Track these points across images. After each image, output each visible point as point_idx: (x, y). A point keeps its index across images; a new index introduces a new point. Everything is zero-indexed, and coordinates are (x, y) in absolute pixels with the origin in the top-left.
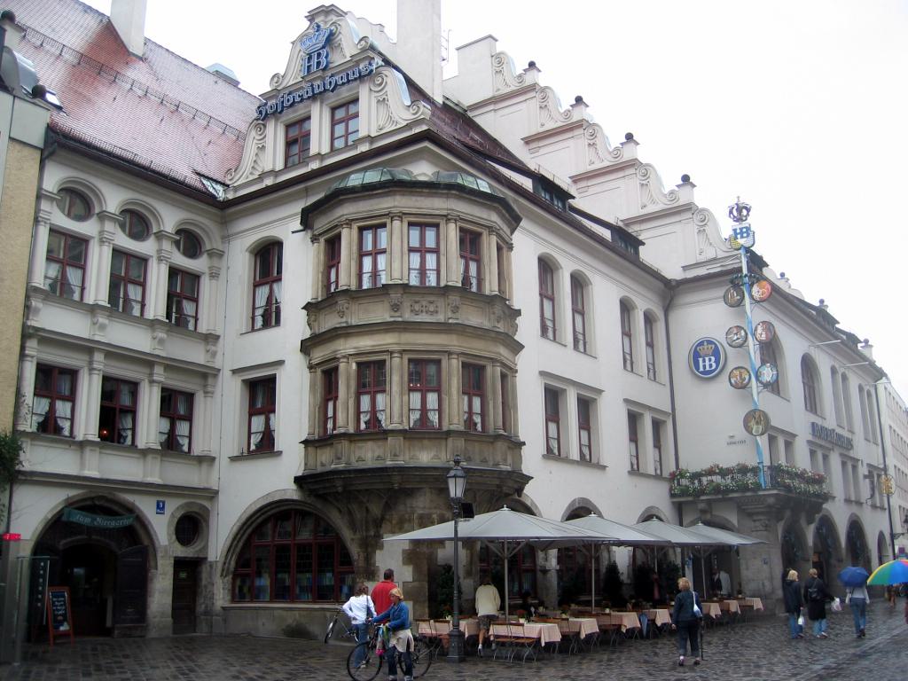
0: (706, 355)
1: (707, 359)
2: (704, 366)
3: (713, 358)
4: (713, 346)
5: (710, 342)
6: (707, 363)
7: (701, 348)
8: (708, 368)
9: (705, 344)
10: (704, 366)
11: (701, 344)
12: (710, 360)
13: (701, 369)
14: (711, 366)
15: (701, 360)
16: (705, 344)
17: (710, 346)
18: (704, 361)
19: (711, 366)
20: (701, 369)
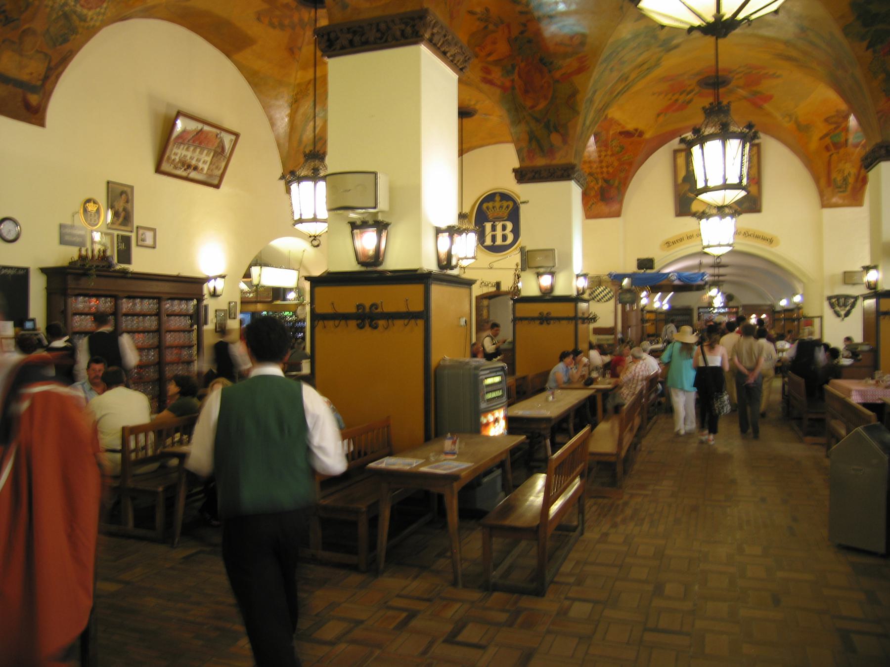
0: (500, 219)
2: (494, 238)
3: (509, 226)
4: (511, 204)
6: (499, 233)
7: (490, 204)
8: (499, 242)
9: (498, 198)
10: (494, 238)
11: (490, 198)
12: (504, 228)
13: (488, 242)
14: (504, 238)
15: (488, 226)
16: (498, 198)
17: (505, 204)
18: (494, 228)
19: (504, 238)
20: (488, 242)
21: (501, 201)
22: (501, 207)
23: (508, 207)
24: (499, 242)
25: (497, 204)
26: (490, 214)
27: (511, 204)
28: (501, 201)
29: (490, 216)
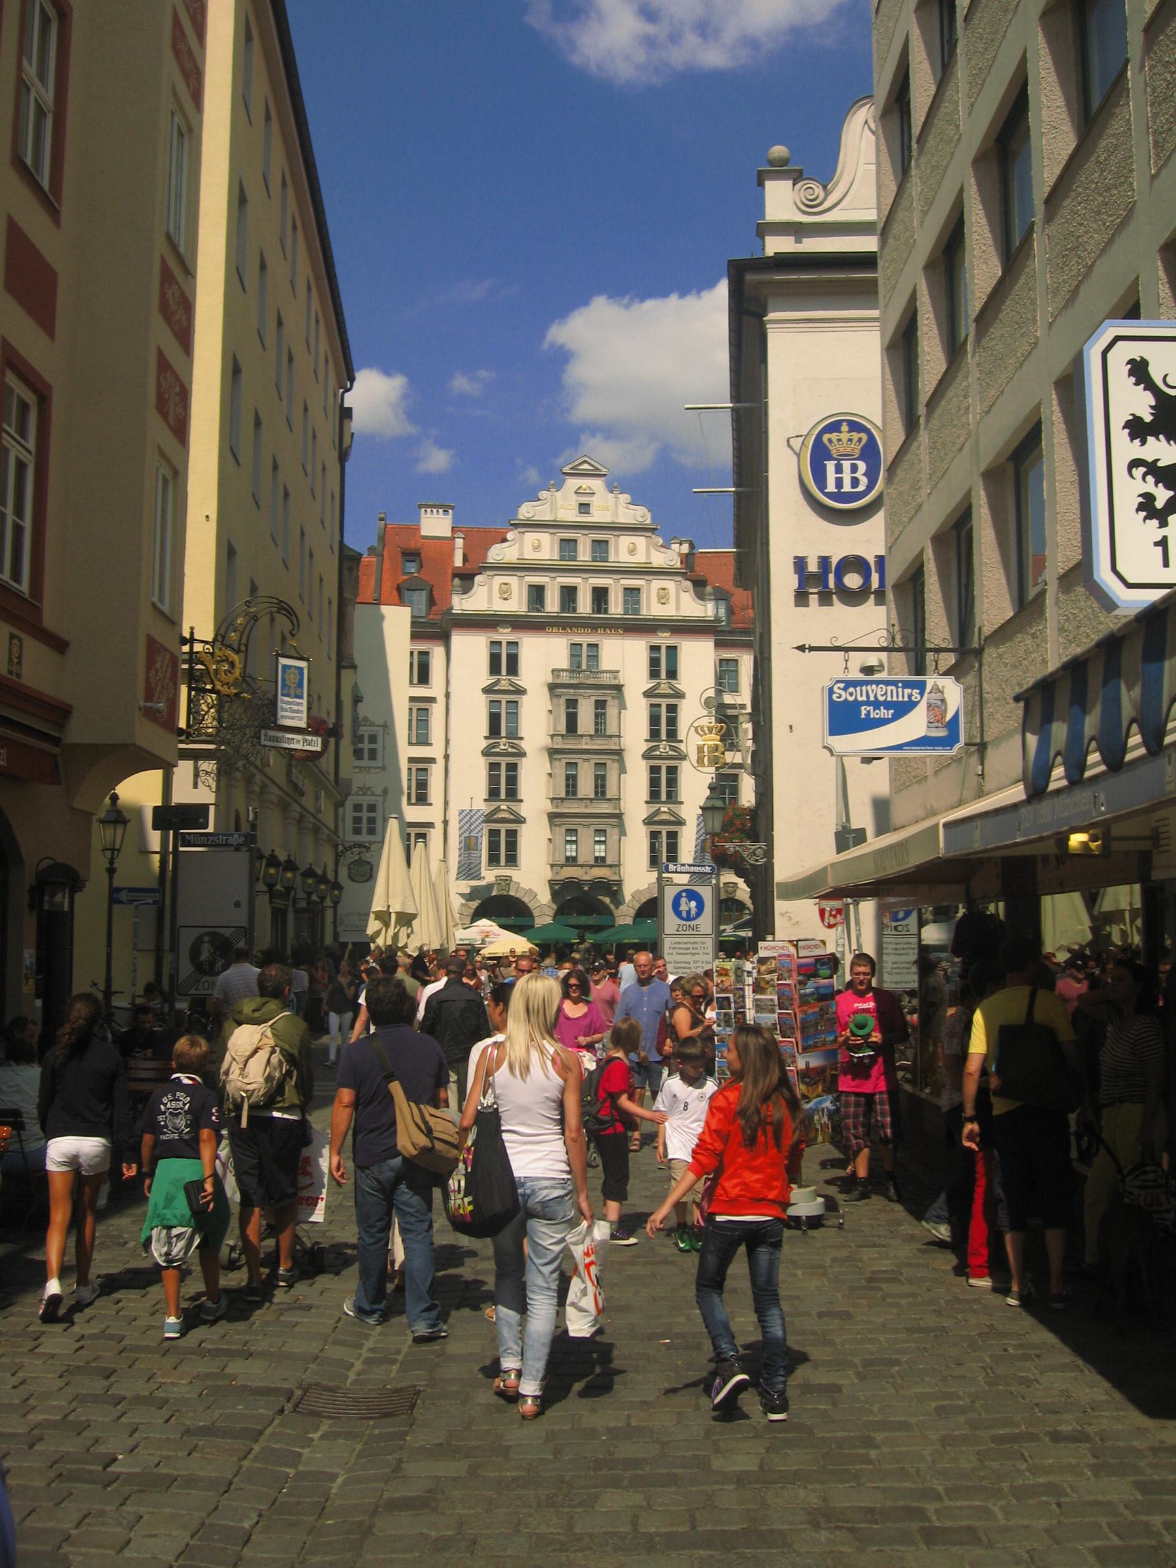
0: (847, 456)
1: (847, 465)
2: (839, 483)
5: (855, 427)
8: (847, 487)
10: (839, 483)
12: (854, 469)
13: (831, 487)
16: (845, 428)
17: (855, 436)
18: (839, 469)
20: (831, 487)
21: (849, 432)
22: (850, 440)
23: (860, 440)
24: (847, 487)
25: (845, 436)
26: (834, 450)
27: (864, 437)
28: (849, 432)
29: (834, 454)
